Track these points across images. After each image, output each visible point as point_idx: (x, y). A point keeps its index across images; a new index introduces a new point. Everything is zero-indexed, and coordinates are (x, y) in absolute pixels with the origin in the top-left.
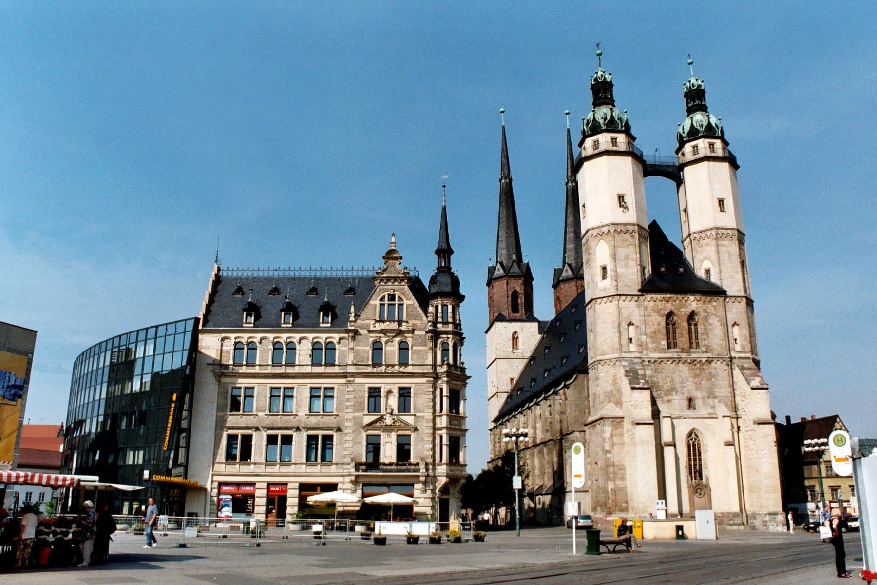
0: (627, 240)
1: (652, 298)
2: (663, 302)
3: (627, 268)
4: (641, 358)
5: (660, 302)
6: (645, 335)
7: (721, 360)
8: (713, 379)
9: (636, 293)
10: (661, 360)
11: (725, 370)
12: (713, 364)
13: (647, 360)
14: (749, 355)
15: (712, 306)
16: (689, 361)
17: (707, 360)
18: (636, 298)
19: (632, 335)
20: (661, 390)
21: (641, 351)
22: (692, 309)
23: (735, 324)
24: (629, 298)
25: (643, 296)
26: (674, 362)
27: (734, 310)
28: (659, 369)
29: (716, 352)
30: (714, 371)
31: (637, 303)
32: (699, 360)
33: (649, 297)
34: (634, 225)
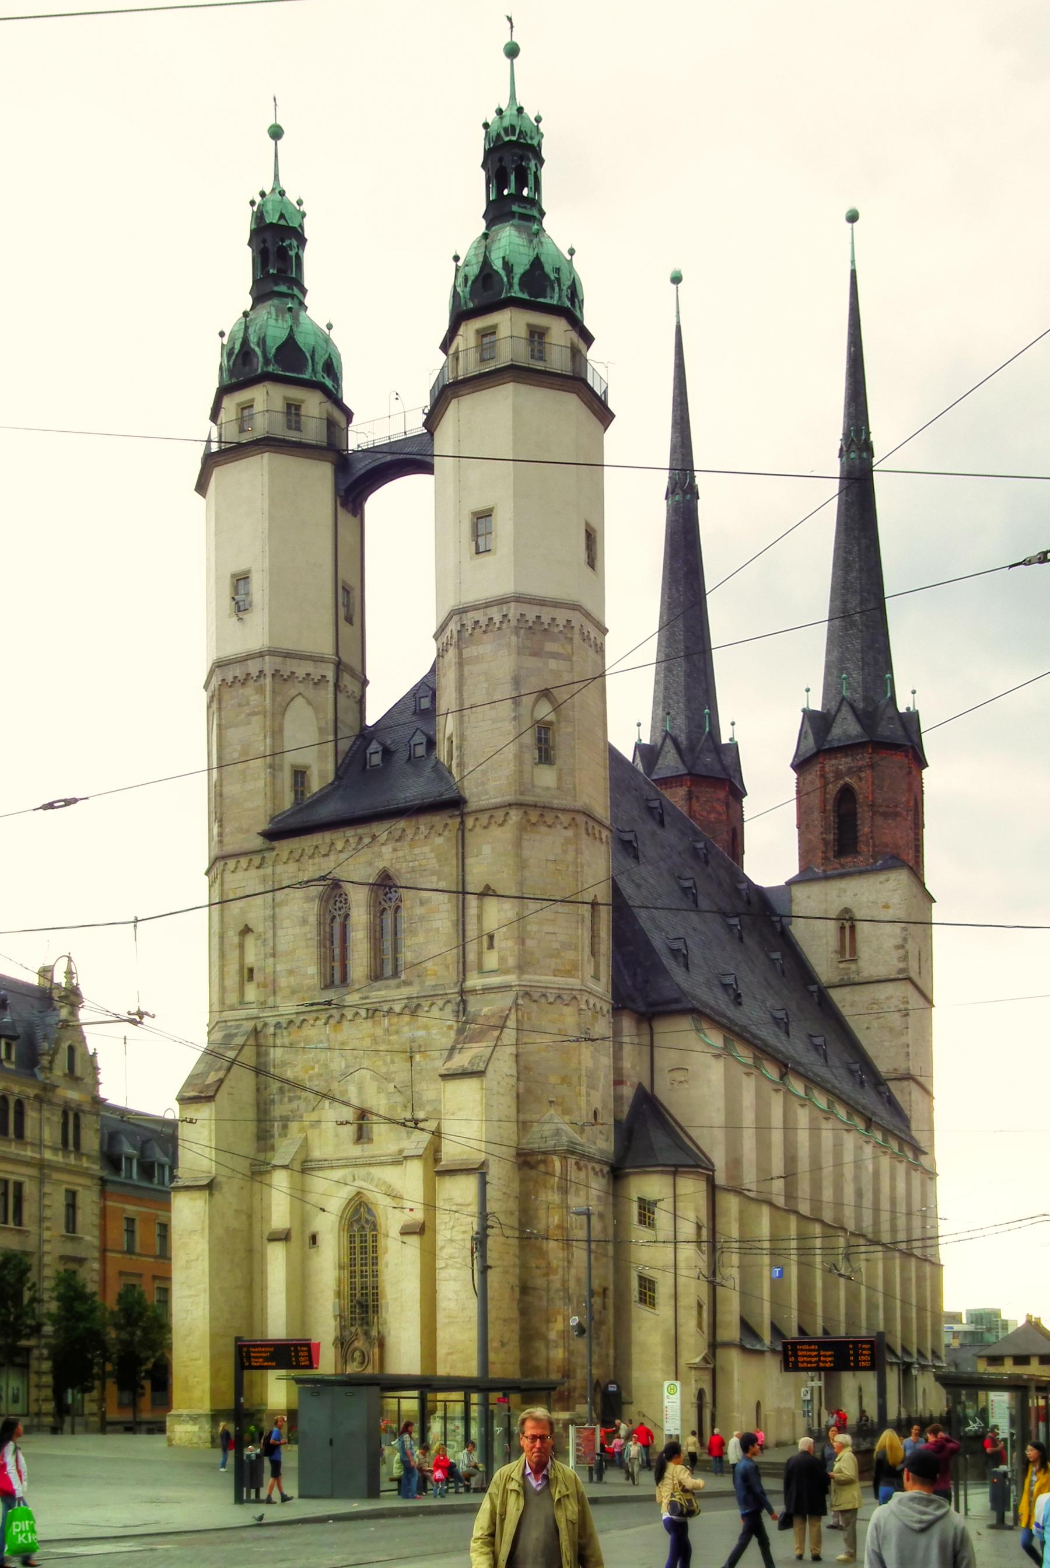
0: (248, 704)
1: (291, 852)
2: (316, 860)
3: (245, 781)
4: (260, 1018)
5: (311, 861)
6: (274, 955)
9: (258, 842)
10: (301, 1018)
11: (450, 1027)
13: (272, 1021)
14: (511, 978)
15: (432, 851)
16: (363, 1013)
17: (406, 1007)
18: (257, 860)
19: (251, 959)
20: (300, 1098)
21: (262, 999)
22: (380, 865)
23: (487, 892)
24: (244, 862)
25: (273, 849)
26: (332, 1021)
27: (487, 849)
28: (298, 1042)
29: (430, 982)
30: (421, 1033)
31: (261, 872)
32: (385, 1008)
33: (285, 846)
34: (261, 655)
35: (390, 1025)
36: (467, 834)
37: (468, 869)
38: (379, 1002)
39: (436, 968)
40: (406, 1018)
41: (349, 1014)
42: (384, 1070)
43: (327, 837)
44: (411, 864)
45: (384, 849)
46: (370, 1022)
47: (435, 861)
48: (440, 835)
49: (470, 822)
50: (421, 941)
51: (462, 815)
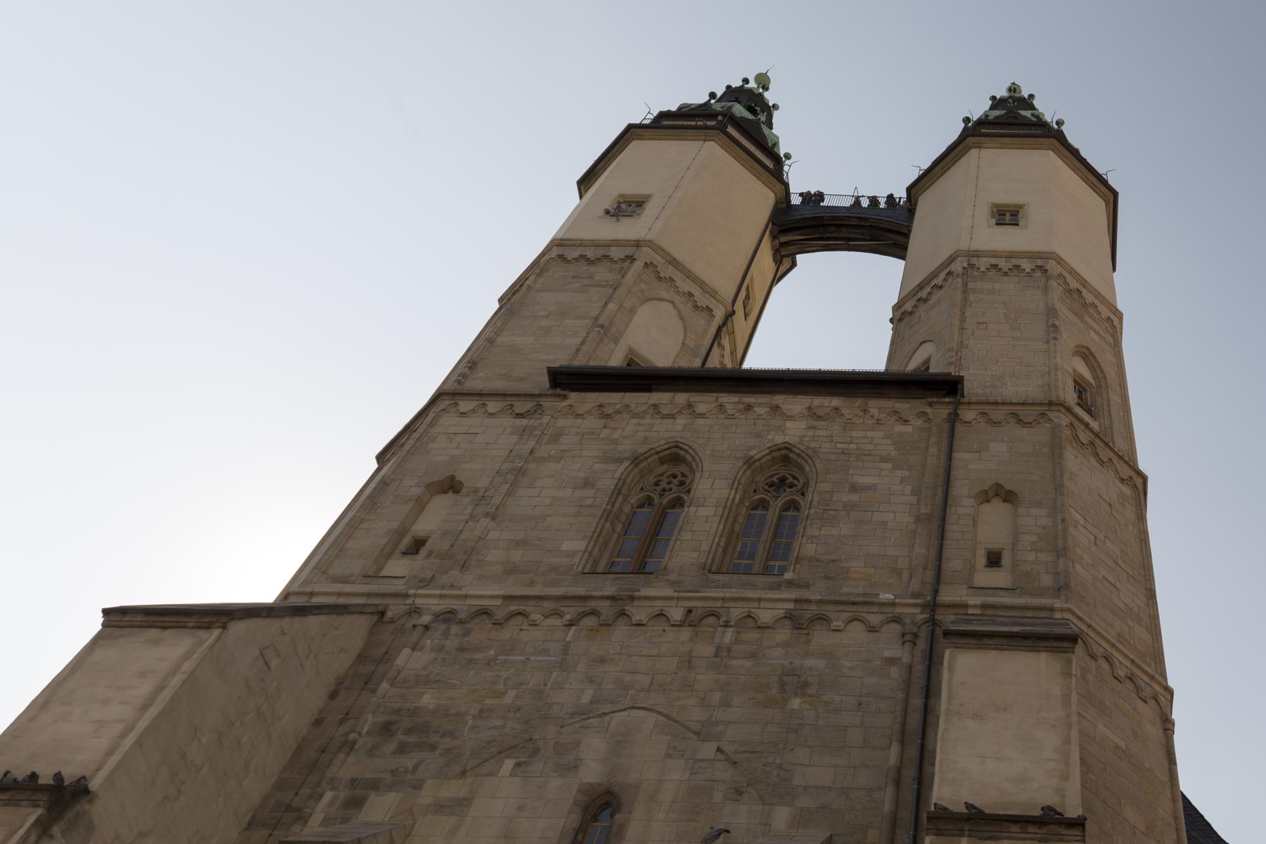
7: (875, 619)
8: (796, 703)
11: (891, 661)
12: (820, 637)
16: (676, 614)
17: (789, 616)
22: (779, 439)
32: (736, 612)
35: (737, 641)
36: (959, 427)
37: (955, 463)
38: (723, 599)
39: (872, 571)
40: (783, 634)
41: (639, 613)
42: (696, 715)
43: (682, 398)
44: (839, 446)
45: (789, 424)
46: (686, 633)
47: (892, 448)
48: (906, 422)
49: (968, 414)
50: (844, 532)
51: (958, 404)
